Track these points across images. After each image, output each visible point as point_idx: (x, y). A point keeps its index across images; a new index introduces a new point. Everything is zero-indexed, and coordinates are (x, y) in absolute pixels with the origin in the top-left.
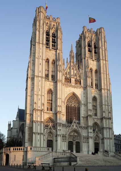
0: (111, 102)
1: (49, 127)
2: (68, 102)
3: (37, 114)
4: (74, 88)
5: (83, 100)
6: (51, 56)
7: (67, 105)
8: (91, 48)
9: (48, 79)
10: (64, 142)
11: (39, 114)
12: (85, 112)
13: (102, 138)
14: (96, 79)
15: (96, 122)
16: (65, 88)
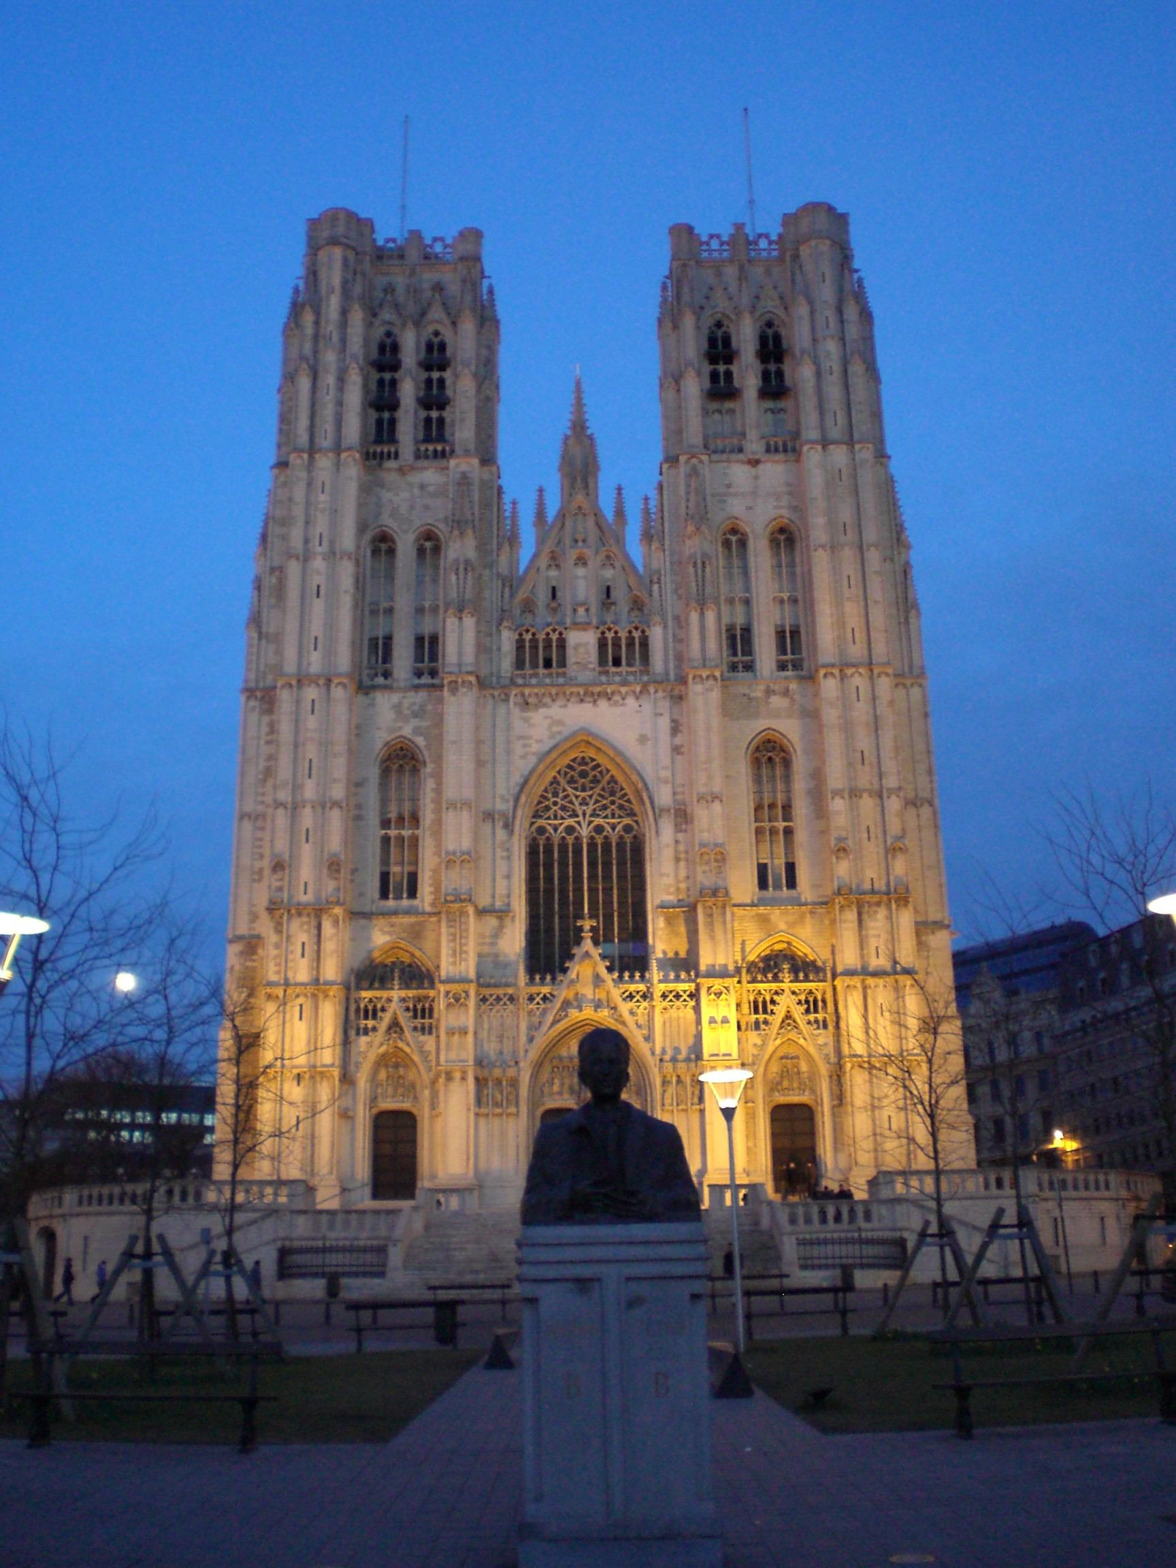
1: (387, 1018)
2: (547, 808)
3: (288, 937)
4: (587, 707)
7: (534, 839)
8: (734, 368)
9: (387, 674)
10: (496, 1122)
14: (785, 595)
16: (516, 712)
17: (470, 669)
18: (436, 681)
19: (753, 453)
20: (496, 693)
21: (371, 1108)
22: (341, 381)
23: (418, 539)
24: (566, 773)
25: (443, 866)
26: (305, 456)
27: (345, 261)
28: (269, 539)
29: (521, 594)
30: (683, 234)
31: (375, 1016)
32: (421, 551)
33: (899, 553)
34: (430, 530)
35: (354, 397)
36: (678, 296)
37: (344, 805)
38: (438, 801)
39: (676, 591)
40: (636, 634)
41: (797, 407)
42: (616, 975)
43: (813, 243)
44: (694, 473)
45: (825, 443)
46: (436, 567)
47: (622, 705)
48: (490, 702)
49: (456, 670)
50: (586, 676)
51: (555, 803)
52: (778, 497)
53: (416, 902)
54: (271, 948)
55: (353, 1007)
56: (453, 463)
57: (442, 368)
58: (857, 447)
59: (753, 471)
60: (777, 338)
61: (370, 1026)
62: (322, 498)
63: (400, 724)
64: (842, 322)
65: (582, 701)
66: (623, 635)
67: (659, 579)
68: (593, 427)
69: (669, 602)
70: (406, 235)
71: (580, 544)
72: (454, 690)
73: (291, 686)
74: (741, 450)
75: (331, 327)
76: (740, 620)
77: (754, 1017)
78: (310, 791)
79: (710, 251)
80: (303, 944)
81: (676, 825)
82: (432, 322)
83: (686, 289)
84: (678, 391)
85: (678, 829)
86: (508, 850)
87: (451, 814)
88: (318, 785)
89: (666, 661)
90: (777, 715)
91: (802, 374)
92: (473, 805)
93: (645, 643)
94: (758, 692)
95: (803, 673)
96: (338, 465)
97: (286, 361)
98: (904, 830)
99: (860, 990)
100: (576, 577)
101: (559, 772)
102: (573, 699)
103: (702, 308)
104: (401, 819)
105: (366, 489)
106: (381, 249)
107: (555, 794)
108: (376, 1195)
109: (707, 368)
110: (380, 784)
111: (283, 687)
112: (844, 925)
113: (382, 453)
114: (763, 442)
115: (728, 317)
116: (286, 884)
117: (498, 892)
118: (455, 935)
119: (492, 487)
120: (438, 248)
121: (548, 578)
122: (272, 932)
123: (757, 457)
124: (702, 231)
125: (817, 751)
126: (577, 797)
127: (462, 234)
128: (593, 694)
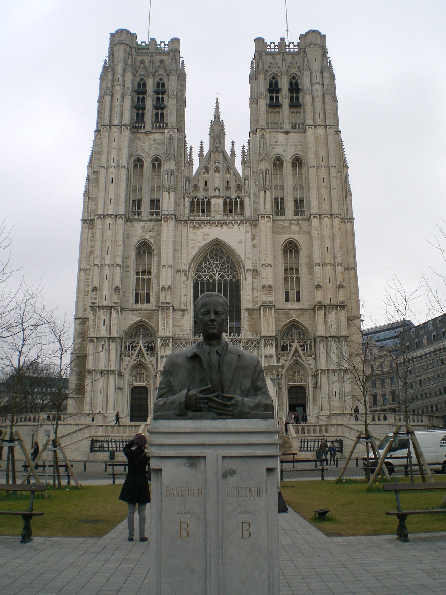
0: (354, 249)
2: (202, 268)
3: (99, 318)
5: (249, 258)
6: (150, 148)
8: (280, 95)
9: (139, 214)
11: (104, 317)
12: (255, 295)
13: (314, 370)
14: (298, 185)
15: (294, 321)
17: (172, 212)
18: (159, 218)
19: (287, 129)
20: (182, 223)
21: (130, 385)
22: (123, 97)
23: (152, 161)
24: (210, 254)
25: (160, 291)
26: (108, 127)
27: (125, 49)
28: (93, 160)
29: (193, 184)
30: (259, 42)
31: (132, 350)
32: (153, 166)
33: (344, 170)
34: (156, 157)
35: (128, 103)
36: (257, 66)
37: (121, 265)
38: (158, 265)
39: (255, 183)
40: (239, 200)
41: (304, 112)
42: (228, 334)
43: (312, 46)
44: (263, 137)
45: (315, 127)
46: (159, 171)
47: (233, 228)
48: (180, 225)
49: (166, 213)
50: (218, 217)
51: (205, 266)
52: (296, 147)
53: (149, 305)
54: (92, 322)
55: (123, 345)
56: (166, 131)
57: (163, 93)
58: (328, 127)
59: (287, 136)
60: (297, 84)
61: (130, 353)
62: (114, 143)
63: (144, 234)
64: (323, 77)
65: (216, 226)
66: (233, 200)
67: (248, 178)
68: (223, 118)
69: (252, 187)
70: (150, 40)
71: (217, 164)
72: (165, 221)
73: (101, 218)
74: (282, 128)
75: (119, 76)
76: (280, 196)
77: (282, 352)
78: (108, 261)
79: (271, 48)
80: (104, 320)
81: (253, 276)
82: (159, 75)
83: (261, 64)
84: (257, 104)
85: (254, 277)
86: (186, 285)
87: (164, 269)
88: (111, 257)
89: (250, 211)
90: (294, 233)
91: (306, 99)
92: (172, 266)
93: (242, 204)
94: (286, 224)
95: (305, 216)
96: (121, 131)
97: (101, 89)
98: (343, 279)
99: (325, 342)
100: (215, 177)
101: (207, 254)
102: (213, 225)
103: (267, 71)
104: (143, 272)
105: (131, 141)
106: (140, 45)
107: (205, 263)
108: (131, 420)
109: (268, 95)
110: (136, 258)
111: (97, 218)
112: (319, 316)
113: (139, 126)
114: (291, 125)
115: (278, 75)
116: (98, 296)
117: (182, 301)
118: (165, 318)
119: (182, 141)
120: (162, 45)
121: (204, 177)
122: (92, 315)
123: (289, 130)
124: (268, 41)
125: (311, 248)
126: (214, 264)
127: (172, 40)
128: (221, 223)
